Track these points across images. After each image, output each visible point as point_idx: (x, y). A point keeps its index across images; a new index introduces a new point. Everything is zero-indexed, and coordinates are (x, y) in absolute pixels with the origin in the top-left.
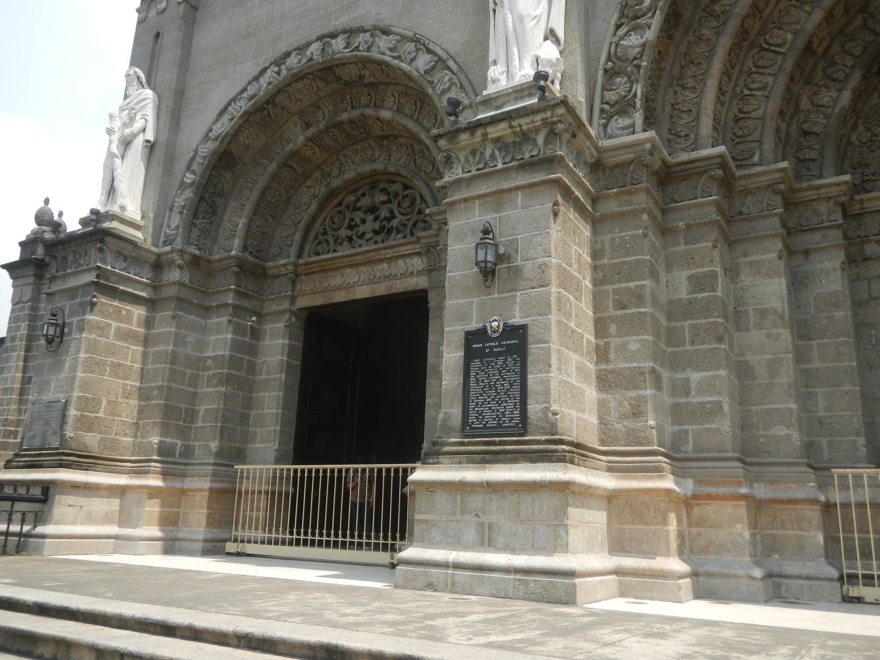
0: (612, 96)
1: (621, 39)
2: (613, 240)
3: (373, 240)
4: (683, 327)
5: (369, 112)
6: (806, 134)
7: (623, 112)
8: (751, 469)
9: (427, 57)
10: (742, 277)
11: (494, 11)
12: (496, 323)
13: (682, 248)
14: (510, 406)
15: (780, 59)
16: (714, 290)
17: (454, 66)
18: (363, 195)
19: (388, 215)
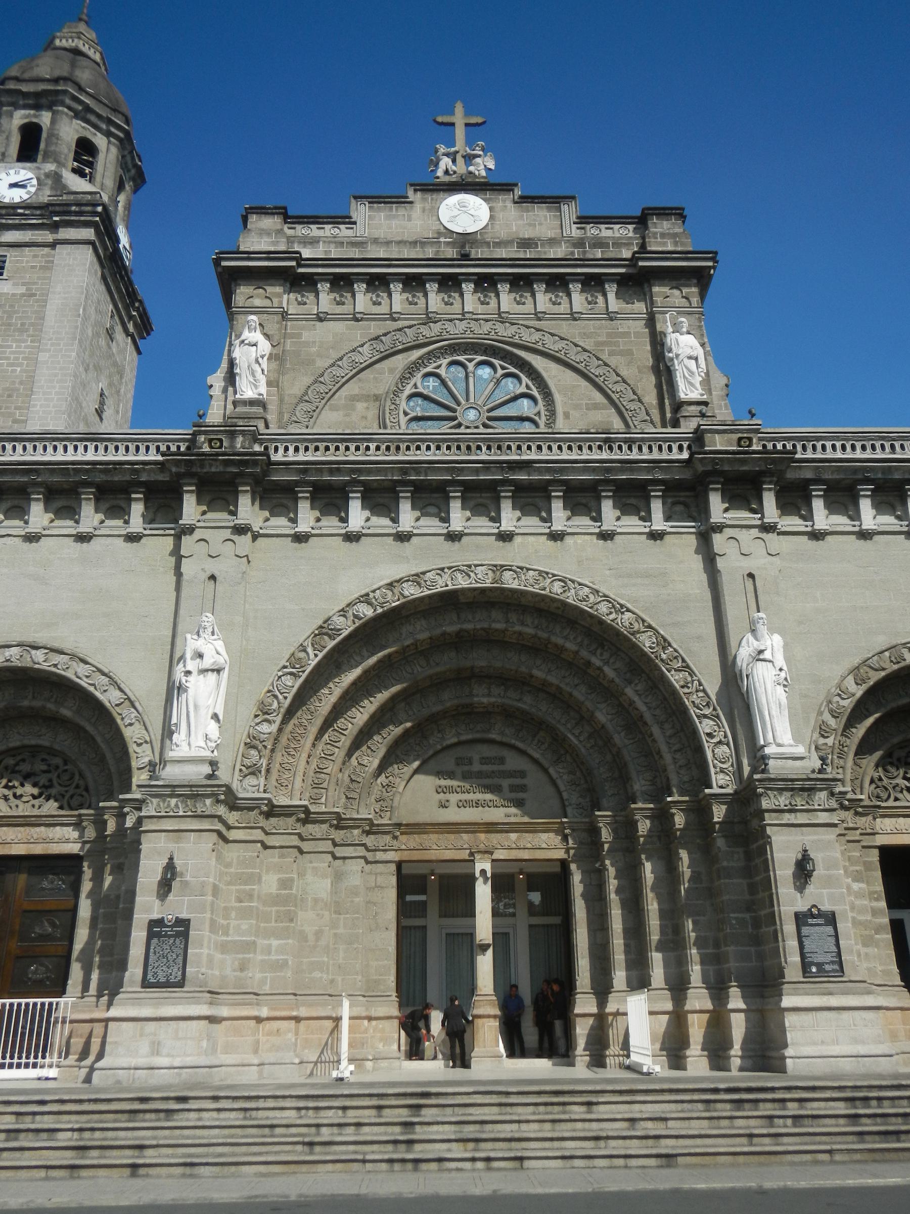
0: (248, 762)
1: (257, 724)
2: (239, 857)
3: (31, 803)
4: (271, 911)
5: (50, 706)
6: (352, 781)
7: (253, 773)
8: (298, 997)
9: (118, 693)
10: (307, 876)
11: (179, 688)
12: (170, 917)
13: (276, 860)
14: (175, 970)
15: (343, 738)
16: (291, 889)
17: (140, 708)
18: (23, 760)
19: (47, 784)
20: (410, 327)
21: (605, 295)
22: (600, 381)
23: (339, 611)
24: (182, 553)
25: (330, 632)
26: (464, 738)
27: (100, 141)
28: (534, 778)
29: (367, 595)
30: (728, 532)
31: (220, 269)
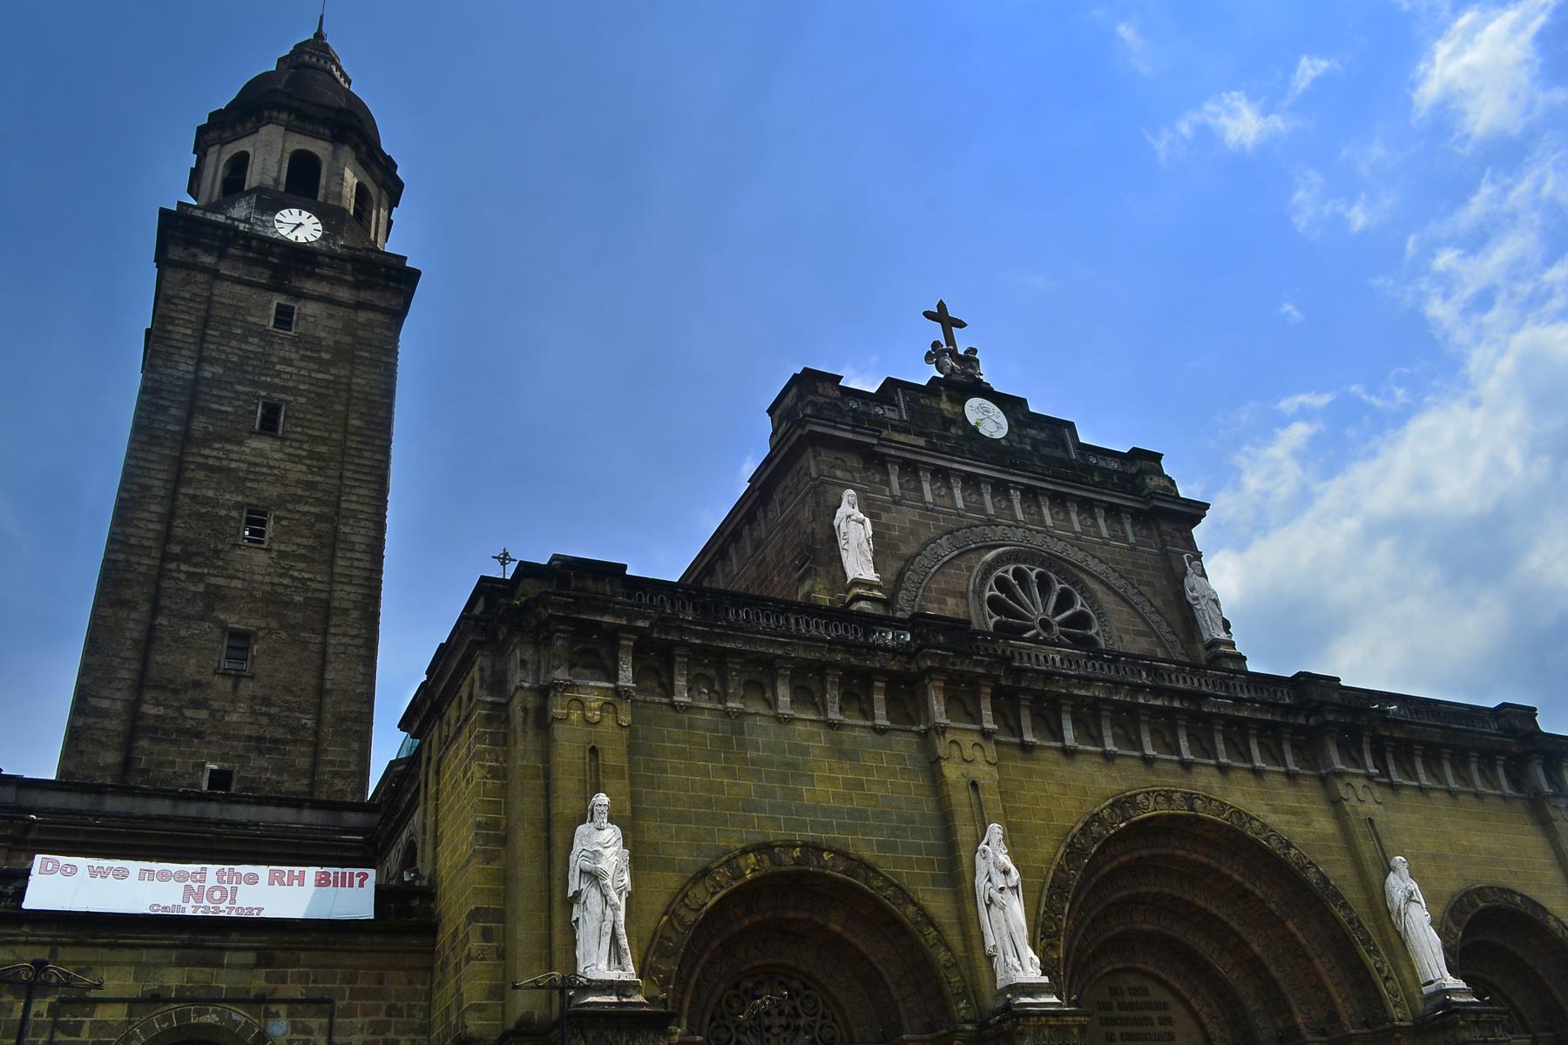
20: (977, 526)
21: (1122, 524)
22: (1139, 607)
23: (1080, 830)
24: (940, 752)
25: (1079, 851)
26: (1117, 966)
27: (373, 189)
28: (1176, 1011)
29: (1097, 814)
30: (1347, 780)
31: (799, 432)
